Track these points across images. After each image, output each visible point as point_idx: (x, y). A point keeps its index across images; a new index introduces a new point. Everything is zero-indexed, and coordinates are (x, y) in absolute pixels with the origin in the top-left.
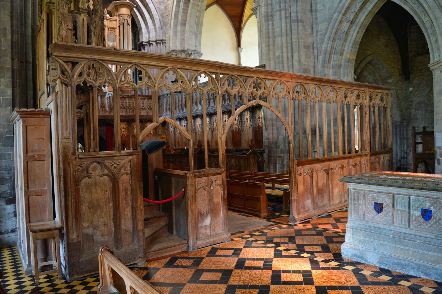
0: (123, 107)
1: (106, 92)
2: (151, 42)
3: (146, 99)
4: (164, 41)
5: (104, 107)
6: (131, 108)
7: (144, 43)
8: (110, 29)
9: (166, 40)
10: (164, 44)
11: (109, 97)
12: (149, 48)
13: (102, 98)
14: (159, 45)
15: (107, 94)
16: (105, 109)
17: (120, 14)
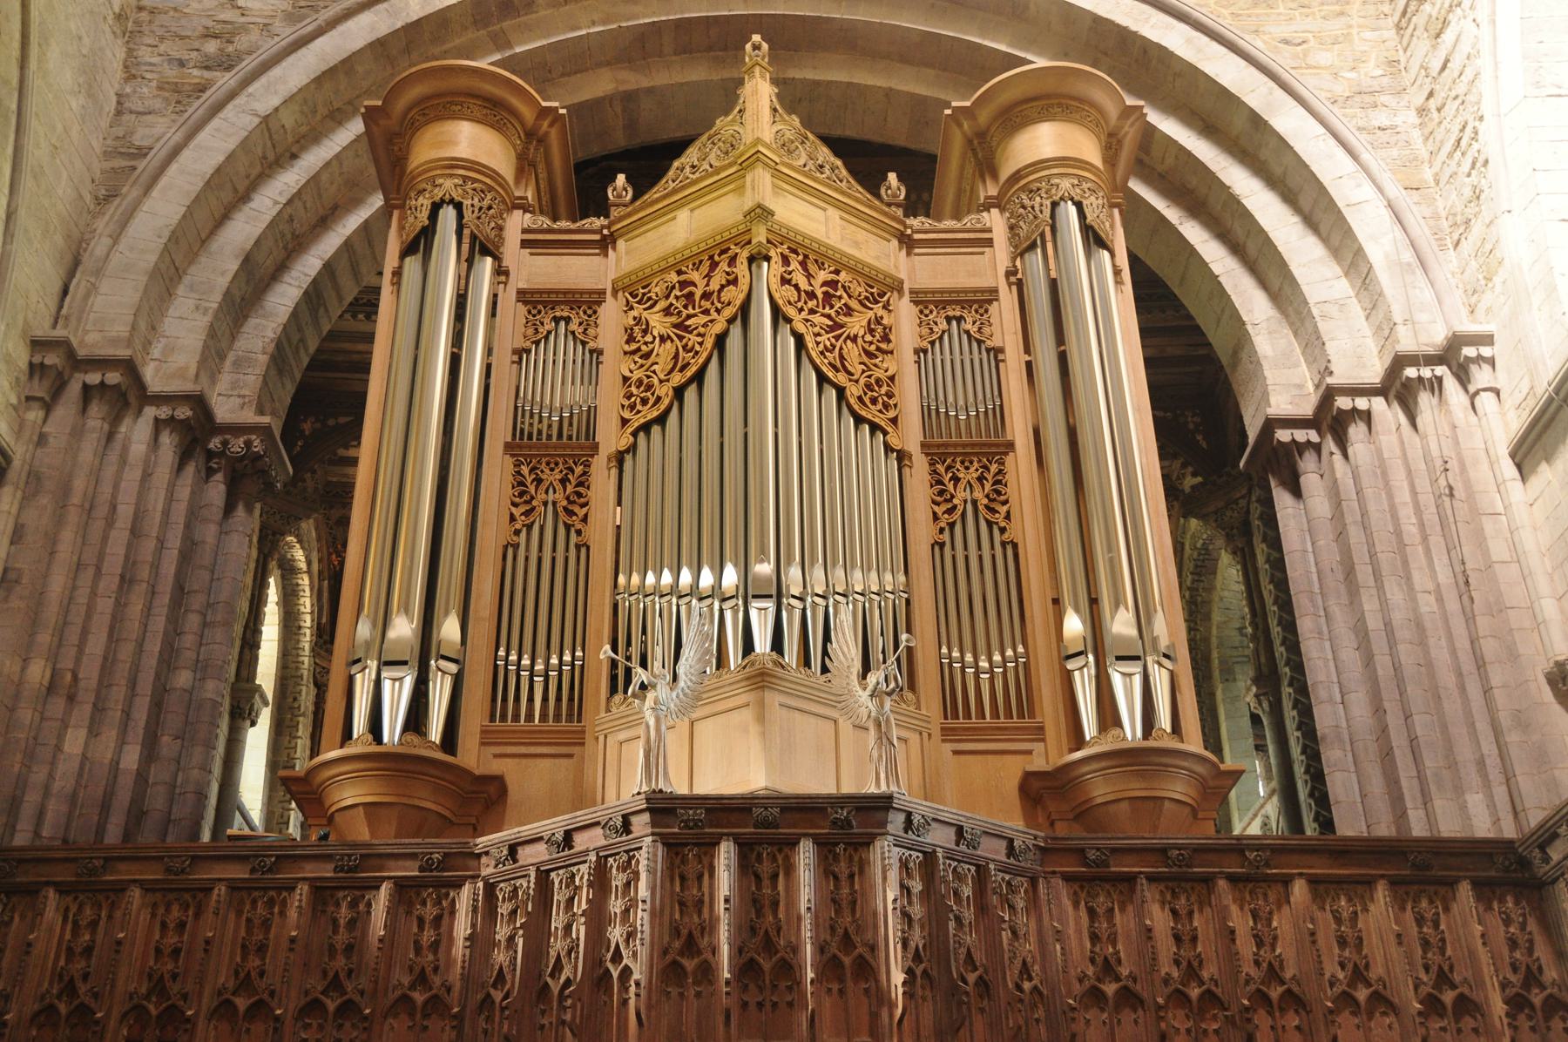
0: (1110, 989)
1: (884, 803)
2: (1343, 403)
3: (1381, 892)
4: (1469, 351)
5: (867, 969)
6: (1210, 997)
7: (1283, 435)
8: (942, 305)
9: (1488, 340)
10: (1481, 377)
11: (929, 857)
12: (1338, 457)
13: (842, 868)
14: (1425, 400)
15: (896, 822)
16: (881, 997)
17: (1016, 176)
